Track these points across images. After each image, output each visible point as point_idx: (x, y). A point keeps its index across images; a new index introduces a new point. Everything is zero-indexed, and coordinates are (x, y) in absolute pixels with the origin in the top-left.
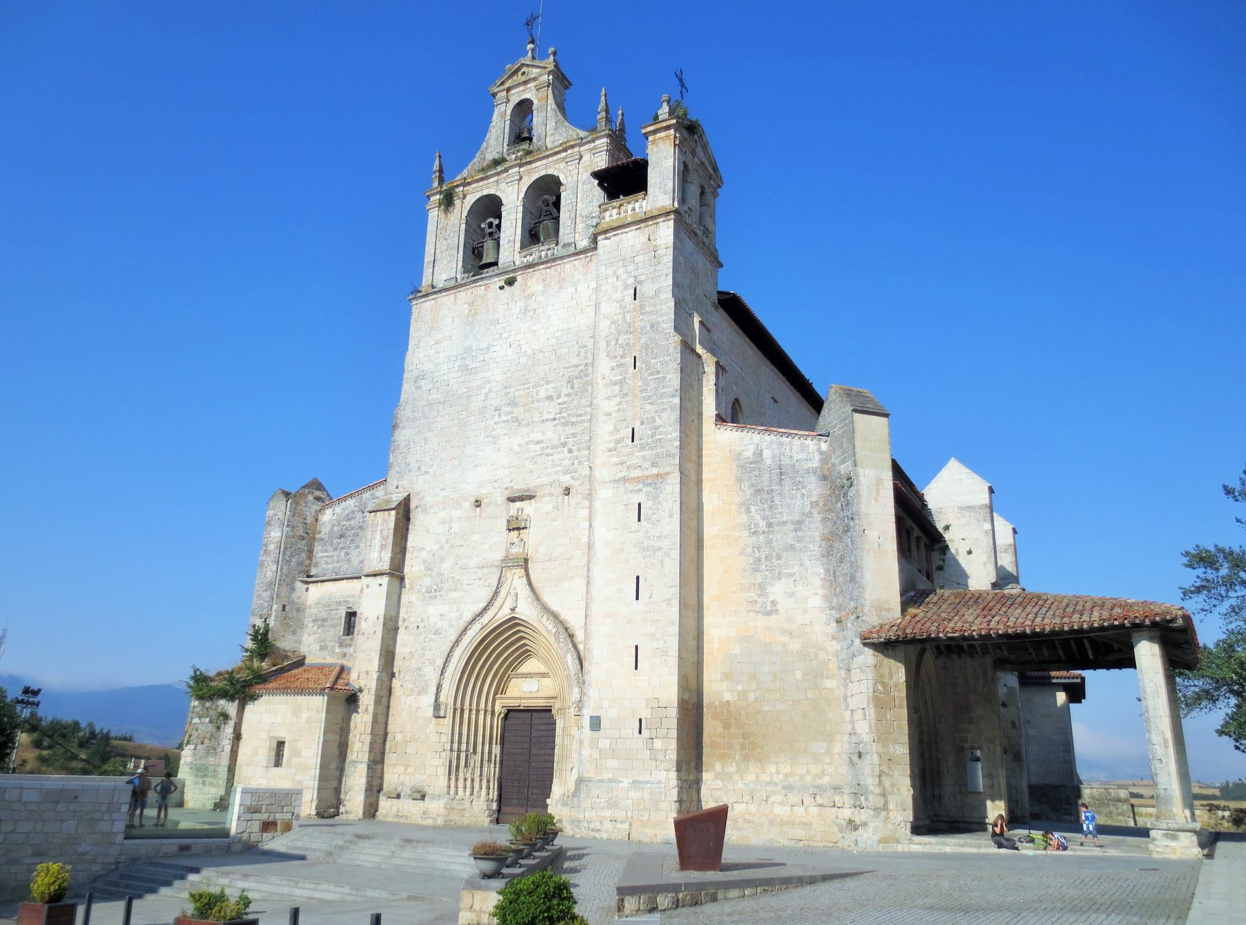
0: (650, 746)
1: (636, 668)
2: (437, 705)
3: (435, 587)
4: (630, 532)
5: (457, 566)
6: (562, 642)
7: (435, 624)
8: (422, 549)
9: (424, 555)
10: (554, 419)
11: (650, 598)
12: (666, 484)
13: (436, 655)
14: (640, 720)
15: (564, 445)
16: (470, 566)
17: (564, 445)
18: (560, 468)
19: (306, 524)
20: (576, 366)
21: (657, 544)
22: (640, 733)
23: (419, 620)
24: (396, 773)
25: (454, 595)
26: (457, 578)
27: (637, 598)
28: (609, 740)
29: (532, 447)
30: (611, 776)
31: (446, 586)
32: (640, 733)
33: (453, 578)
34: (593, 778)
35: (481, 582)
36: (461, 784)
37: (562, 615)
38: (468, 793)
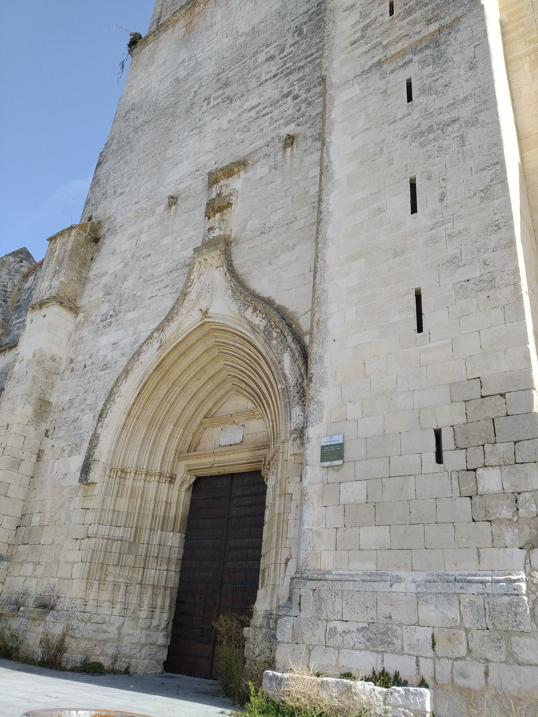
0: (468, 489)
1: (420, 329)
2: (86, 469)
3: (112, 313)
4: (394, 122)
5: (141, 280)
6: (276, 339)
7: (105, 356)
8: (105, 273)
9: (105, 280)
10: (275, 76)
11: (441, 200)
12: (457, 32)
13: (99, 396)
14: (438, 434)
15: (286, 96)
16: (155, 276)
17: (286, 96)
18: (281, 121)
19: (6, 291)
20: (306, 12)
21: (454, 114)
22: (439, 459)
23: (87, 356)
24: (22, 576)
25: (131, 315)
26: (138, 294)
27: (414, 210)
28: (364, 483)
29: (246, 116)
30: (370, 567)
31: (124, 308)
32: (439, 459)
33: (134, 295)
34: (329, 572)
35: (167, 290)
36: (105, 596)
37: (276, 301)
38: (116, 612)
